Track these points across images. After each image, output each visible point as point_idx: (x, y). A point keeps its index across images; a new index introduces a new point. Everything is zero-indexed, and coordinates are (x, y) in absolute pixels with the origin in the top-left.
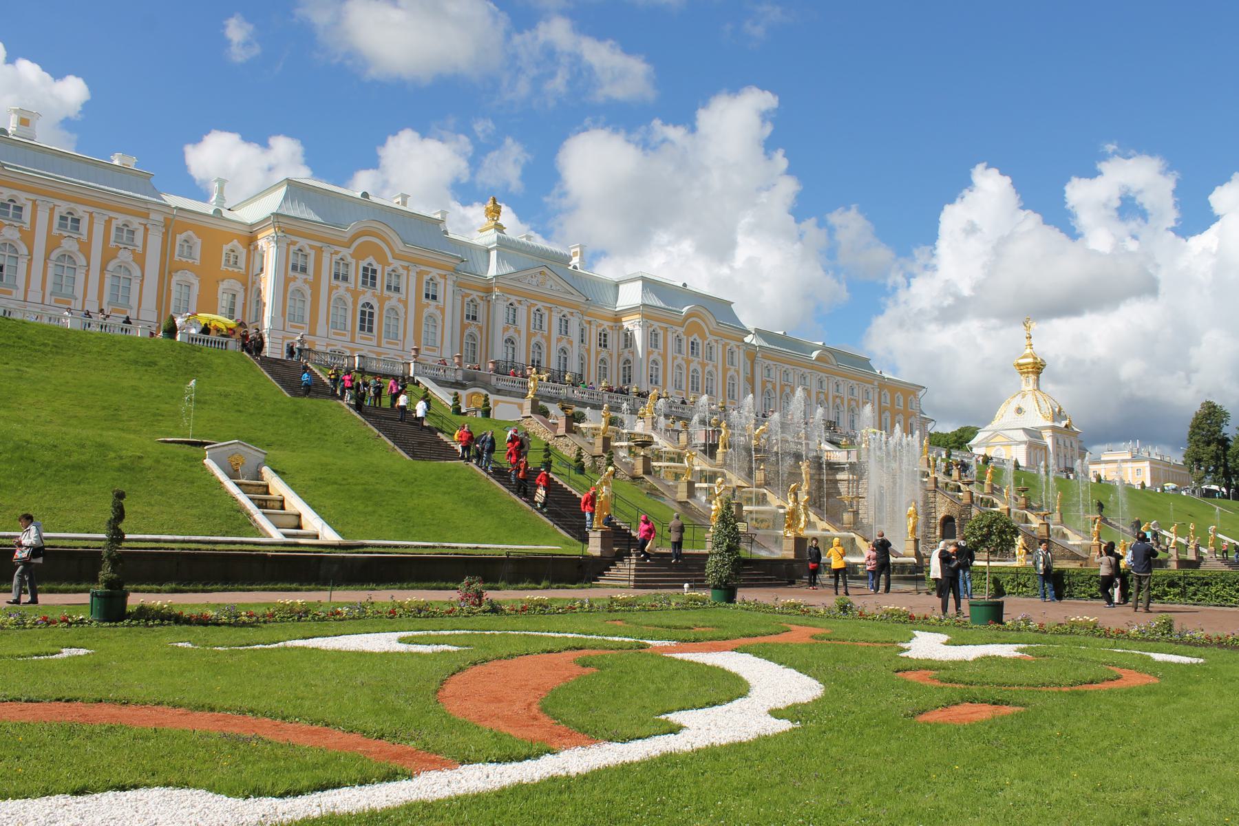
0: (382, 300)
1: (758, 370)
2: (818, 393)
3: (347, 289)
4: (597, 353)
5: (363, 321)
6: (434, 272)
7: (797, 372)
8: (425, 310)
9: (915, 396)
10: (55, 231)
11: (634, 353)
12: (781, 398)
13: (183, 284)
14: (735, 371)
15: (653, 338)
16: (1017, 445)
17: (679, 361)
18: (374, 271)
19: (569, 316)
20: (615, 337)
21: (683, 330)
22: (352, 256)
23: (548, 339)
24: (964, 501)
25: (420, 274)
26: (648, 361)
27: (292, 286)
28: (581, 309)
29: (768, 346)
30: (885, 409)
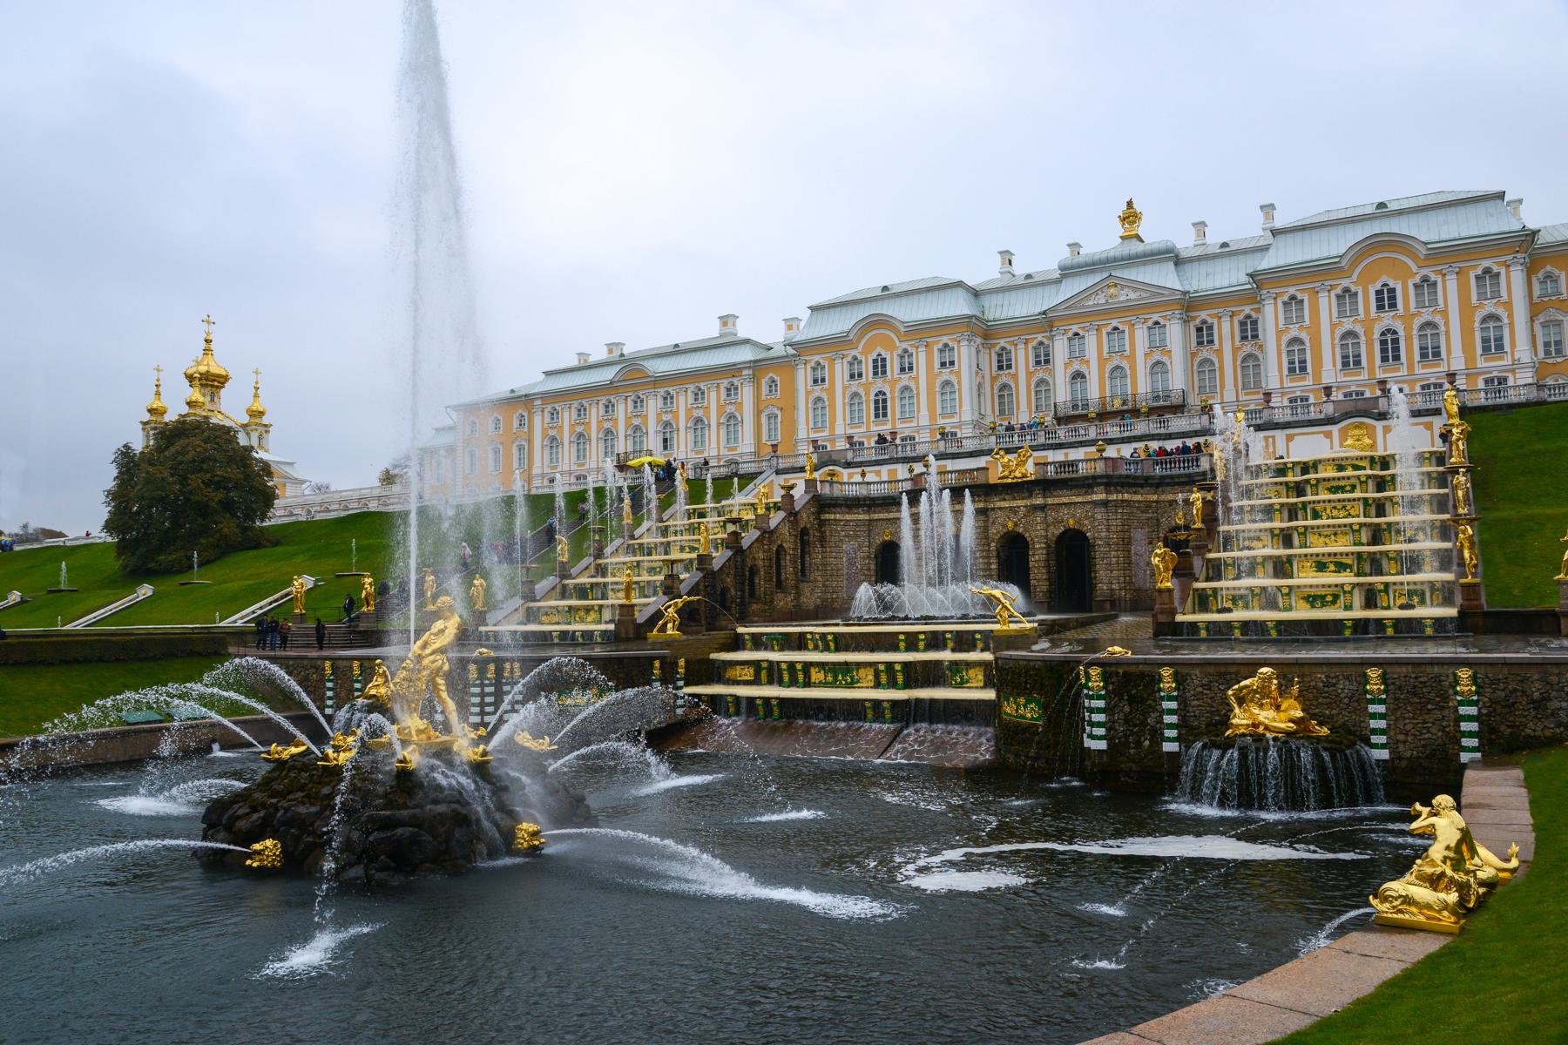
0: (893, 382)
5: (877, 409)
6: (945, 339)
17: (1348, 325)
18: (884, 360)
19: (1162, 322)
22: (860, 353)
23: (1132, 358)
26: (1279, 345)
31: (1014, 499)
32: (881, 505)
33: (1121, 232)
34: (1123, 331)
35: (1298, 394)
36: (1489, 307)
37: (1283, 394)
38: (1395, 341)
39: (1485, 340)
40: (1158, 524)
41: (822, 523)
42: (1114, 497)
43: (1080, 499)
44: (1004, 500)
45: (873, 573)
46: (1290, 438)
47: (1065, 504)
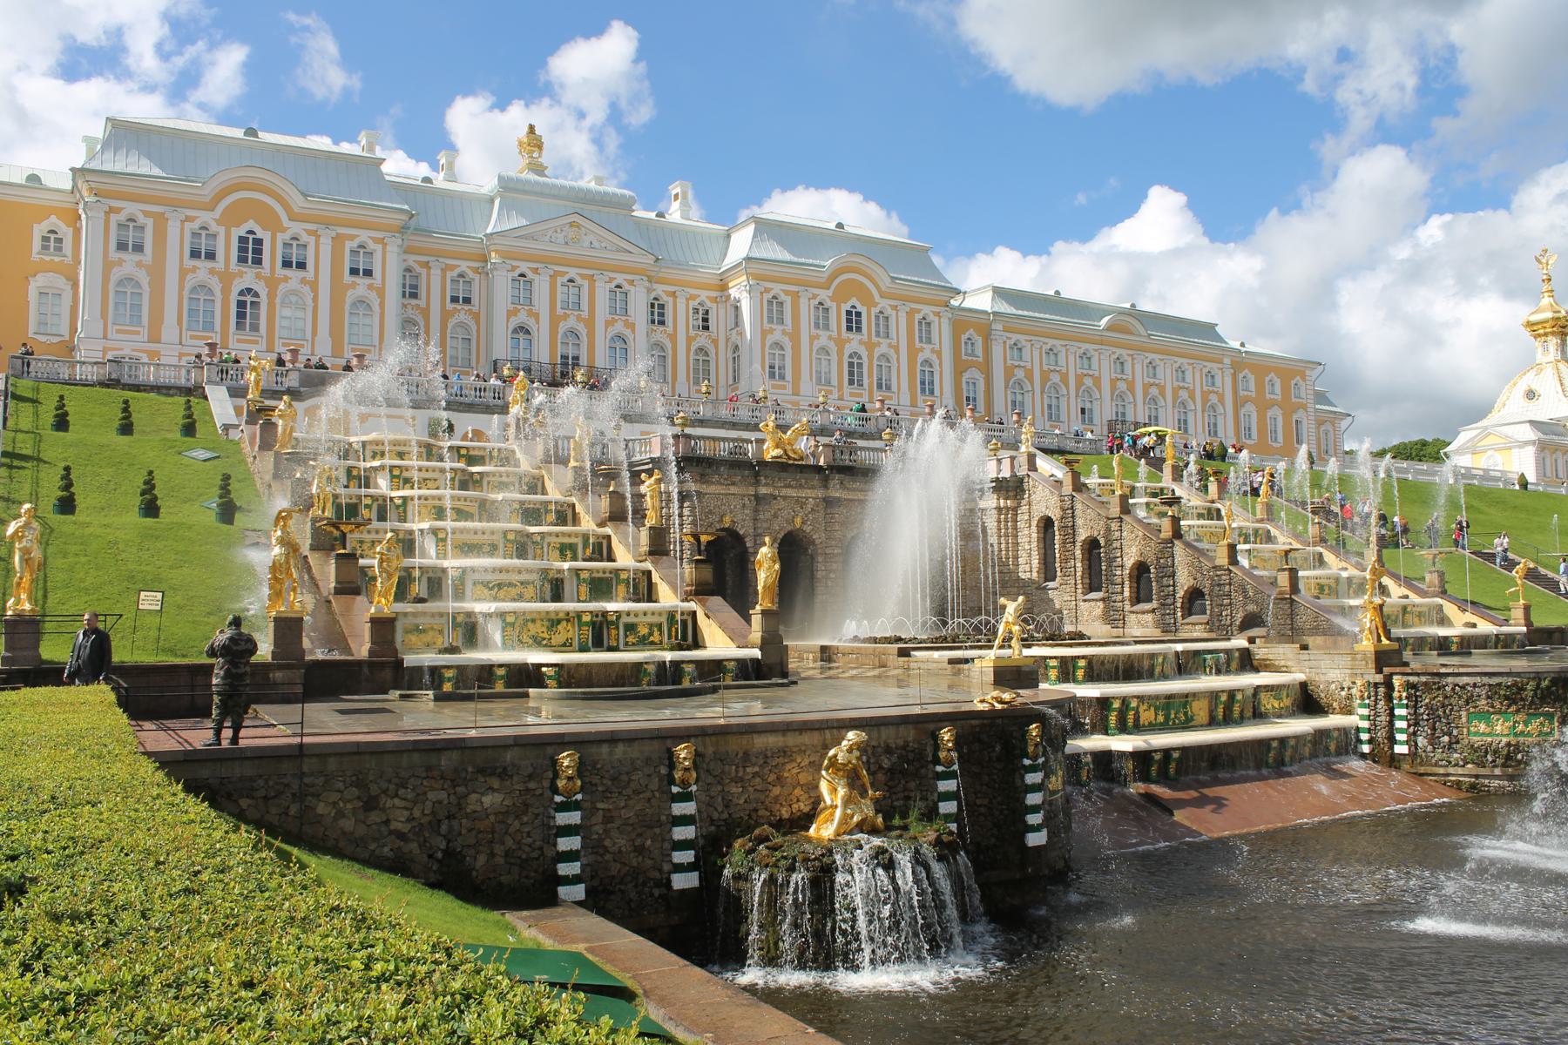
0: (272, 284)
1: (997, 351)
2: (1113, 382)
4: (689, 340)
6: (364, 236)
7: (1072, 350)
8: (349, 293)
9: (1304, 378)
11: (741, 334)
12: (1042, 392)
13: (50, 291)
14: (933, 351)
15: (773, 309)
16: (1520, 447)
18: (259, 242)
19: (626, 286)
20: (722, 312)
21: (830, 293)
22: (219, 222)
23: (590, 323)
24: (1163, 535)
25: (338, 240)
27: (116, 275)
28: (649, 273)
29: (1014, 311)
30: (1247, 400)
31: (801, 486)
36: (926, 354)
38: (860, 365)
39: (923, 383)
44: (789, 486)
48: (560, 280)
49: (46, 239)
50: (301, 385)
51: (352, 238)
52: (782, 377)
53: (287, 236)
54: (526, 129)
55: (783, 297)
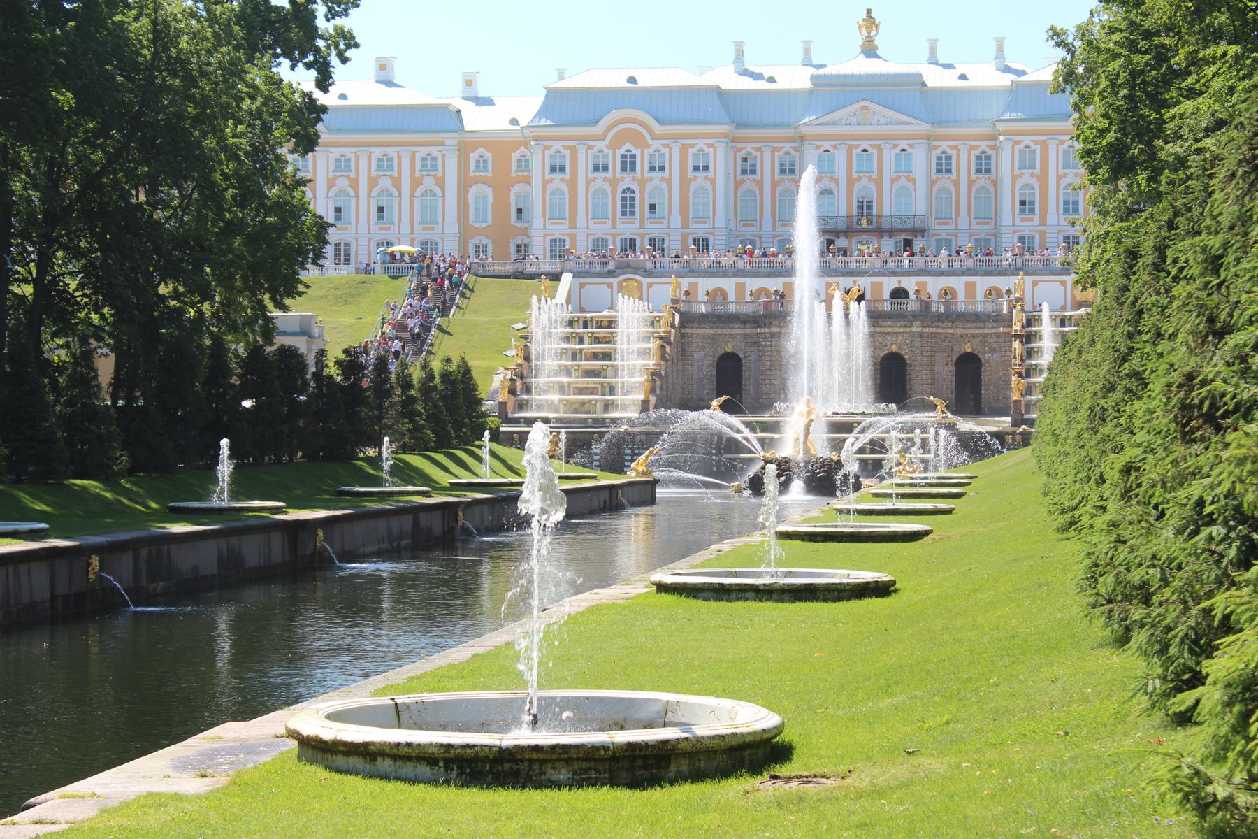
0: (643, 183)
3: (605, 180)
4: (971, 183)
5: (624, 206)
6: (701, 143)
10: (374, 174)
18: (633, 156)
19: (909, 150)
22: (608, 147)
23: (879, 182)
25: (684, 149)
27: (550, 188)
32: (724, 322)
33: (860, 41)
34: (872, 154)
35: (1027, 232)
37: (1014, 232)
40: (952, 350)
41: (683, 335)
42: (926, 330)
43: (901, 330)
45: (714, 378)
46: (1035, 284)
47: (889, 333)
48: (855, 152)
49: (519, 161)
50: (617, 268)
51: (693, 146)
52: (1032, 211)
53: (651, 150)
54: (864, 16)
55: (1033, 146)
